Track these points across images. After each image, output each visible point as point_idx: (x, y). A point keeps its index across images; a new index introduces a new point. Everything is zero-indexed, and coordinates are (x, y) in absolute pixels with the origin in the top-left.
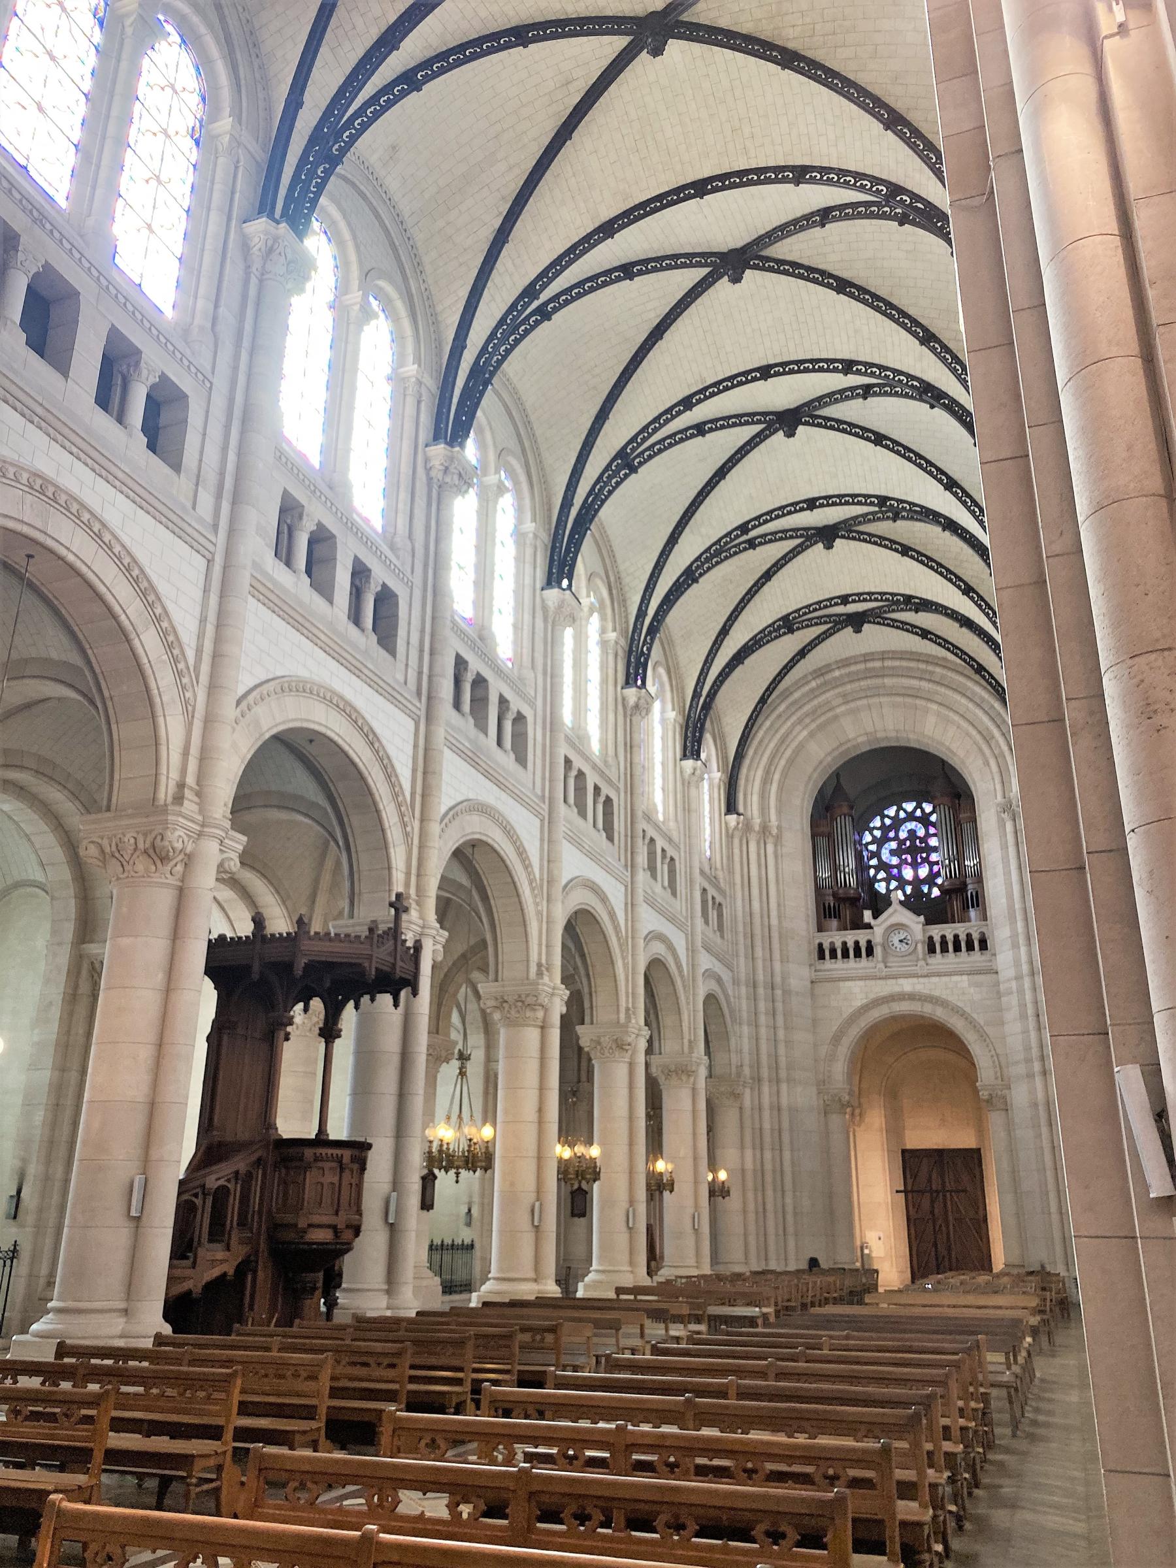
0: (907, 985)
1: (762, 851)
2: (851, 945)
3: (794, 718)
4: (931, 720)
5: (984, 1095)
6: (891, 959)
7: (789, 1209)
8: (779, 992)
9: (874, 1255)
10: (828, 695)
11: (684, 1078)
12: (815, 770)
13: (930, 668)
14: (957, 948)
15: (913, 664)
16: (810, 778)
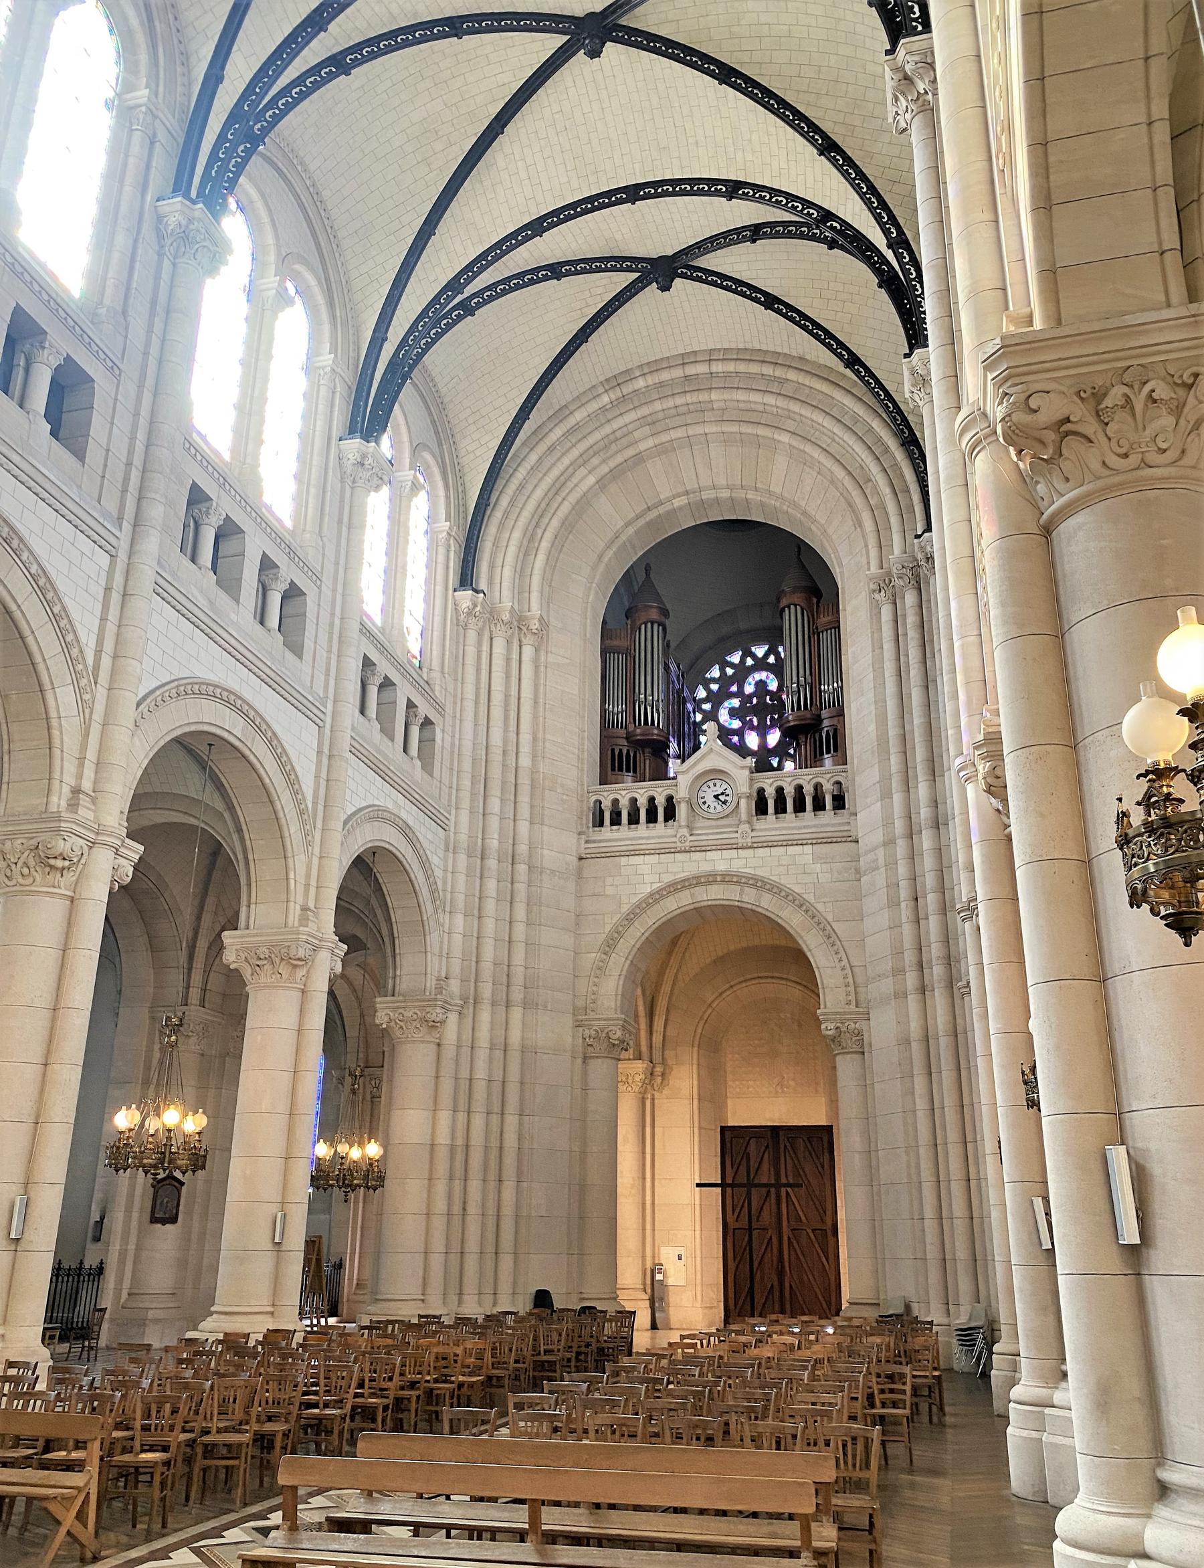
0: (720, 862)
1: (515, 656)
2: (642, 803)
3: (575, 453)
4: (781, 462)
5: (828, 1028)
6: (700, 823)
7: (508, 1211)
8: (522, 868)
9: (670, 1281)
10: (629, 417)
11: (284, 970)
12: (608, 547)
13: (779, 372)
14: (800, 807)
15: (754, 368)
16: (600, 557)
